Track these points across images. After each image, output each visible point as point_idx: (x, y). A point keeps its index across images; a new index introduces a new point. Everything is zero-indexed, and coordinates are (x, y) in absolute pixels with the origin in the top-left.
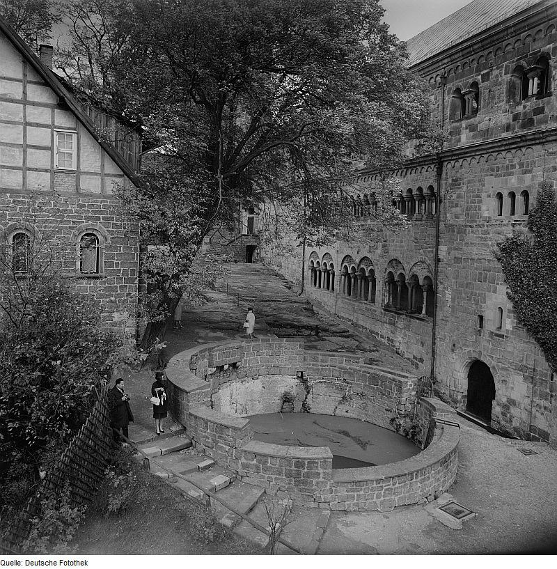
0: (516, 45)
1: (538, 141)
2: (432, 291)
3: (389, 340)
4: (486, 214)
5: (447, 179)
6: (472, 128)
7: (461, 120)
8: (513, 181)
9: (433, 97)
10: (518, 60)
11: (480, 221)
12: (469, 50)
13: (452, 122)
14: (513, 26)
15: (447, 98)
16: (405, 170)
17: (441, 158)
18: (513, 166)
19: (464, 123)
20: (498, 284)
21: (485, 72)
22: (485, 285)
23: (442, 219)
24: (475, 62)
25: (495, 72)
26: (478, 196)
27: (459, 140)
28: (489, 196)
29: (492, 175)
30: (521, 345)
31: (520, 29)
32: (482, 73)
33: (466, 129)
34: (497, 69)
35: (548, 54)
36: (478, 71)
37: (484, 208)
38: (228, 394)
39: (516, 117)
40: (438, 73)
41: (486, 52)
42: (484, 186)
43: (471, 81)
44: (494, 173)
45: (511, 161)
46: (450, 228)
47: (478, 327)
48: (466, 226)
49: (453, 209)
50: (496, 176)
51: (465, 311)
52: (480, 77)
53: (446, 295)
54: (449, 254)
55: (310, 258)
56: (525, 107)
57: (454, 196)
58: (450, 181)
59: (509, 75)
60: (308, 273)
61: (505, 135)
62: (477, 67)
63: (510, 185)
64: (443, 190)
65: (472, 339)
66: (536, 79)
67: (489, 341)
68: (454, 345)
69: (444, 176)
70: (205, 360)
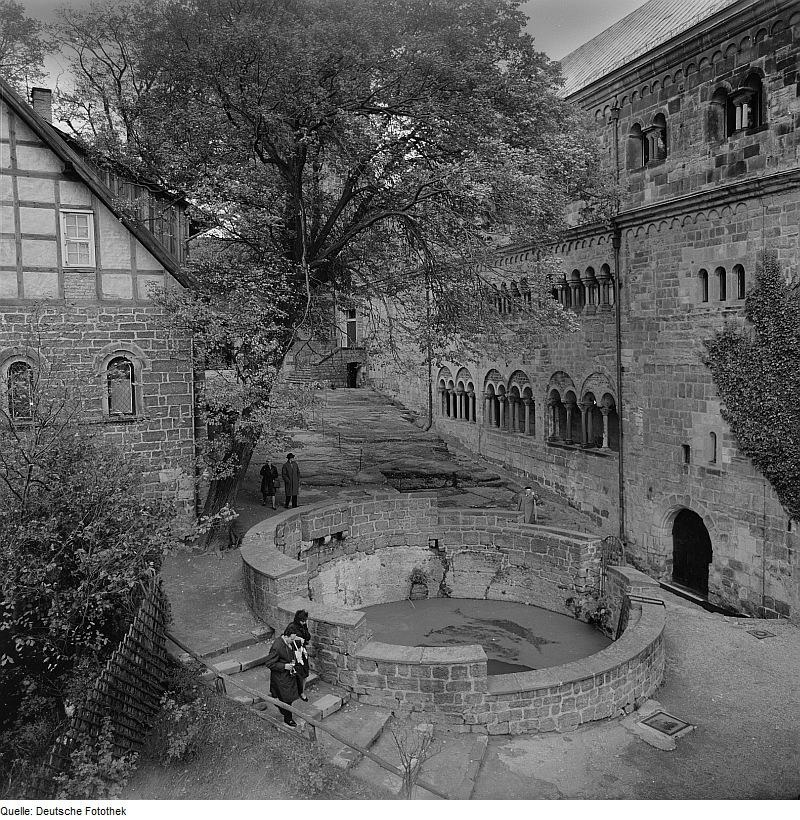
0: (715, 60)
1: (752, 194)
2: (615, 415)
3: (557, 486)
4: (685, 301)
5: (627, 254)
6: (660, 179)
7: (643, 169)
8: (721, 251)
9: (601, 138)
10: (718, 80)
11: (677, 311)
12: (648, 69)
13: (632, 172)
14: (709, 33)
15: (621, 139)
16: (568, 244)
17: (618, 224)
18: (720, 231)
19: (648, 173)
20: (707, 399)
21: (673, 99)
22: (690, 401)
23: (623, 310)
24: (658, 86)
25: (688, 99)
26: (674, 276)
27: (642, 198)
28: (688, 275)
29: (691, 245)
30: (745, 484)
31: (719, 37)
32: (669, 100)
33: (652, 180)
34: (691, 93)
35: (760, 69)
36: (664, 97)
37: (682, 292)
38: (333, 577)
39: (720, 162)
40: (606, 104)
41: (674, 71)
42: (680, 260)
43: (654, 112)
44: (694, 242)
45: (717, 223)
46: (636, 322)
47: (683, 461)
48: (658, 319)
49: (639, 297)
50: (696, 246)
51: (663, 439)
52: (666, 107)
53: (635, 419)
54: (636, 360)
55: (439, 377)
56: (732, 146)
57: (640, 277)
58: (632, 256)
59: (707, 102)
60: (438, 399)
61: (707, 187)
62: (661, 93)
63: (717, 259)
64: (623, 270)
65: (675, 478)
66: (745, 106)
67: (699, 481)
68: (650, 490)
69: (623, 249)
70: (297, 531)
